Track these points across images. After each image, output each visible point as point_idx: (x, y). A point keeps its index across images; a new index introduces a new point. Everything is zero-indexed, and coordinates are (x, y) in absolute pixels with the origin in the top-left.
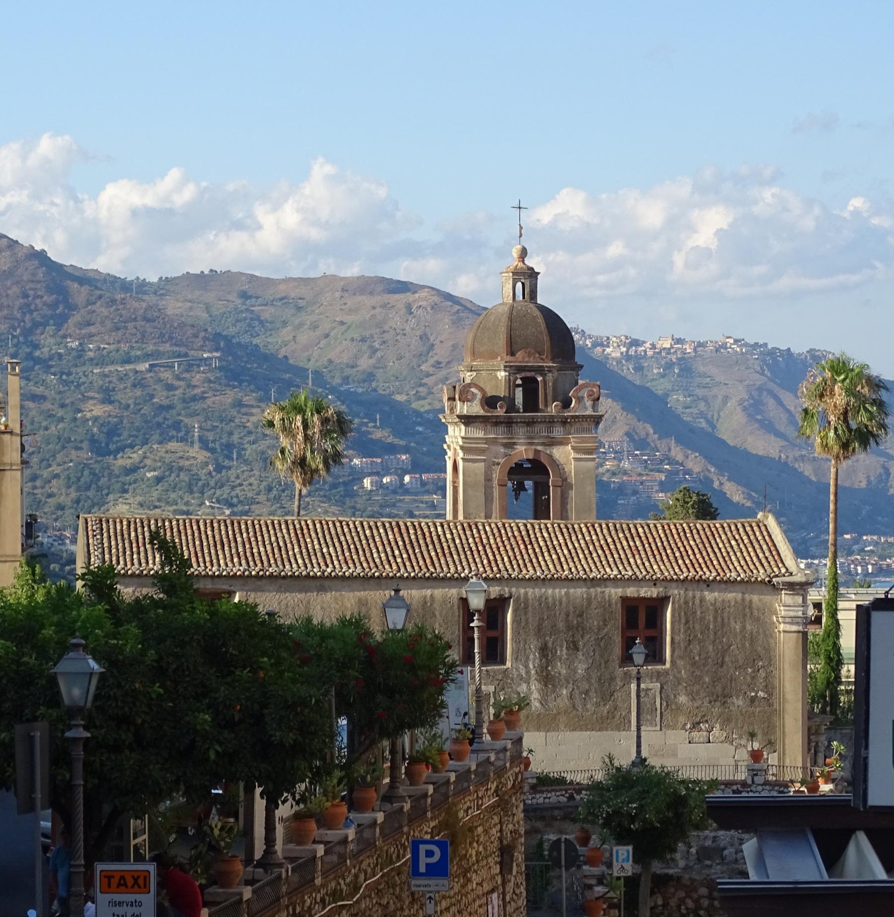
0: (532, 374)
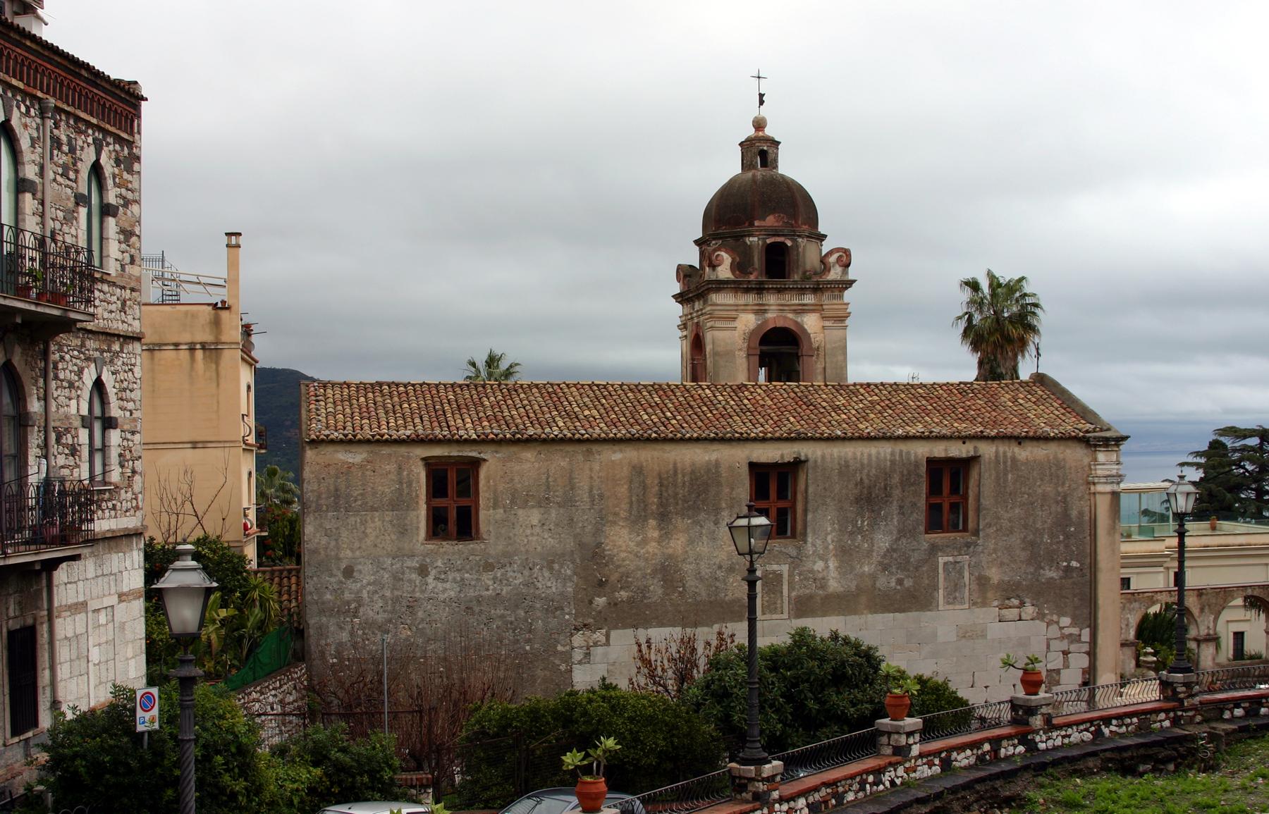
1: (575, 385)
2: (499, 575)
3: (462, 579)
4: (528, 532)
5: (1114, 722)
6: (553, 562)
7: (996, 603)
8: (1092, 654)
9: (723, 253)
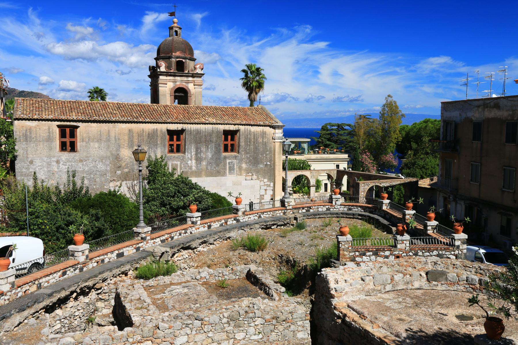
1: (112, 103)
2: (84, 163)
3: (72, 165)
4: (94, 150)
5: (265, 213)
6: (103, 160)
7: (244, 175)
8: (274, 190)
9: (163, 64)
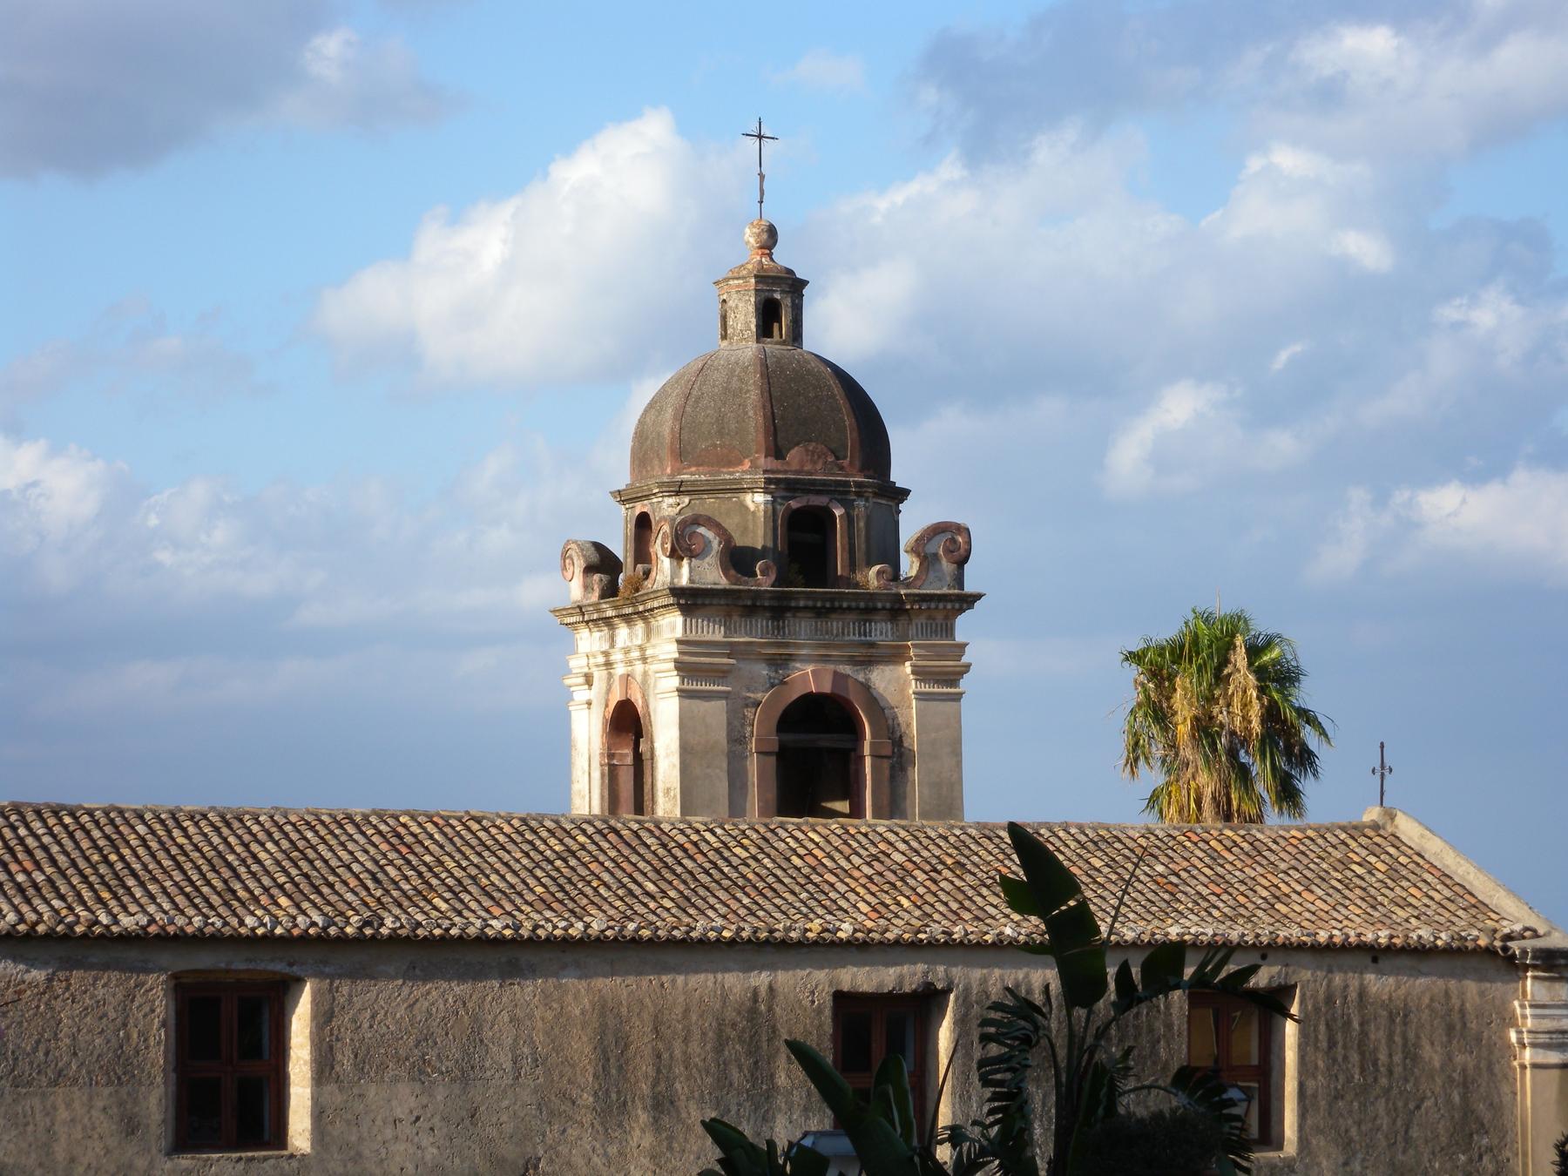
0: (819, 501)
4: (389, 1133)
